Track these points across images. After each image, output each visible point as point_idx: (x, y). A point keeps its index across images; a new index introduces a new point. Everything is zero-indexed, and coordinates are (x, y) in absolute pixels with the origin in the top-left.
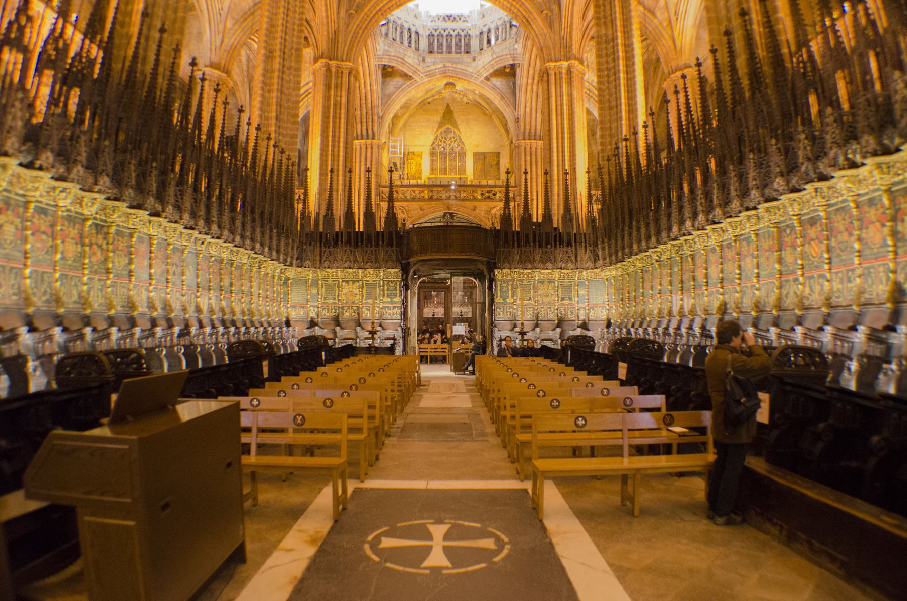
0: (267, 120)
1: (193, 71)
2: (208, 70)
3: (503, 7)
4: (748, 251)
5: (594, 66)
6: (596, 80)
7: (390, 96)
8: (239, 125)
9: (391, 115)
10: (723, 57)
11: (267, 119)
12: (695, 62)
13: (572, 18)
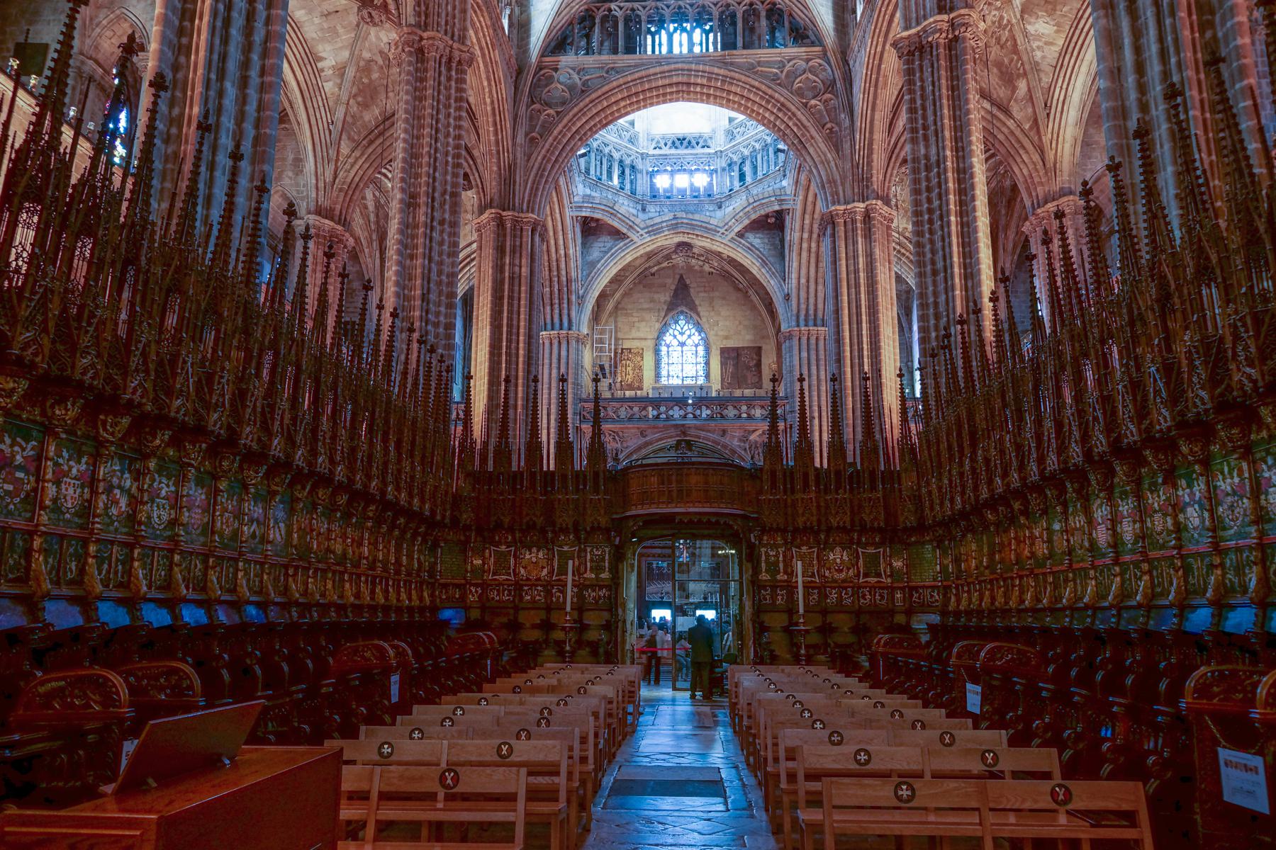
0: (409, 301)
1: (289, 222)
2: (312, 219)
3: (762, 121)
4: (1192, 494)
5: (908, 205)
6: (910, 227)
7: (592, 264)
8: (364, 309)
9: (597, 294)
10: (1134, 174)
11: (407, 298)
12: (1080, 188)
13: (871, 132)
